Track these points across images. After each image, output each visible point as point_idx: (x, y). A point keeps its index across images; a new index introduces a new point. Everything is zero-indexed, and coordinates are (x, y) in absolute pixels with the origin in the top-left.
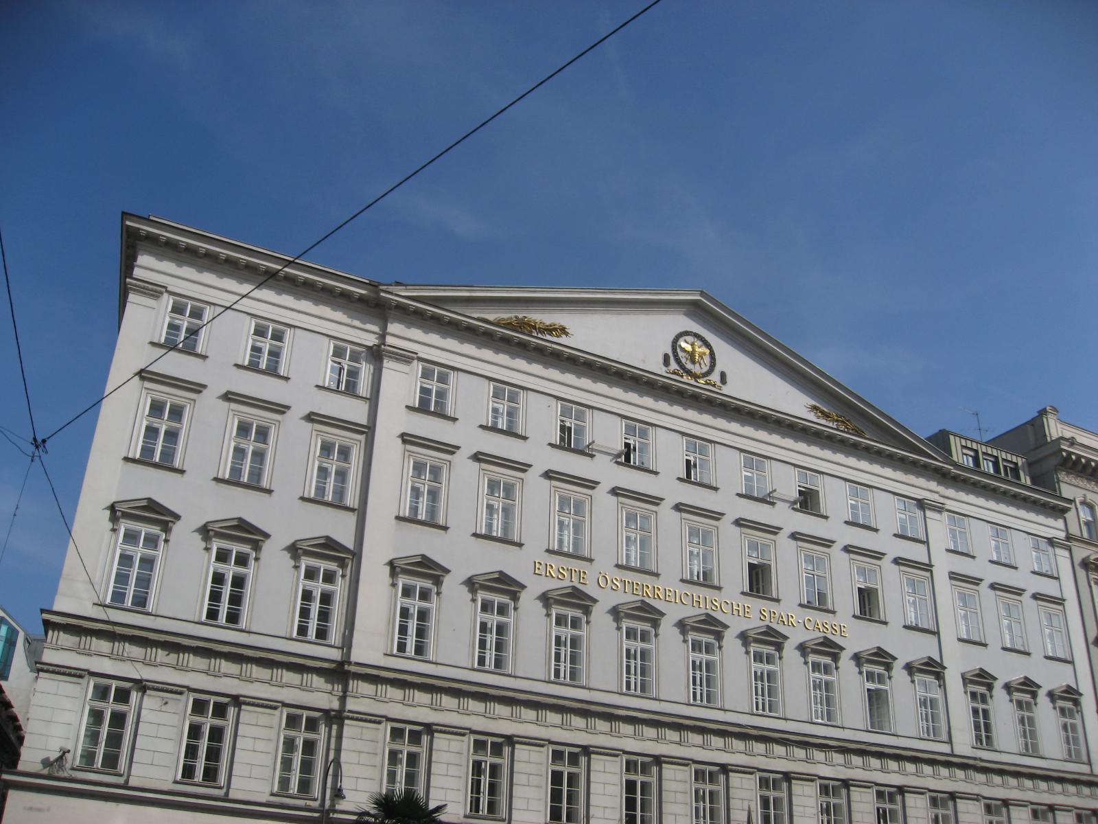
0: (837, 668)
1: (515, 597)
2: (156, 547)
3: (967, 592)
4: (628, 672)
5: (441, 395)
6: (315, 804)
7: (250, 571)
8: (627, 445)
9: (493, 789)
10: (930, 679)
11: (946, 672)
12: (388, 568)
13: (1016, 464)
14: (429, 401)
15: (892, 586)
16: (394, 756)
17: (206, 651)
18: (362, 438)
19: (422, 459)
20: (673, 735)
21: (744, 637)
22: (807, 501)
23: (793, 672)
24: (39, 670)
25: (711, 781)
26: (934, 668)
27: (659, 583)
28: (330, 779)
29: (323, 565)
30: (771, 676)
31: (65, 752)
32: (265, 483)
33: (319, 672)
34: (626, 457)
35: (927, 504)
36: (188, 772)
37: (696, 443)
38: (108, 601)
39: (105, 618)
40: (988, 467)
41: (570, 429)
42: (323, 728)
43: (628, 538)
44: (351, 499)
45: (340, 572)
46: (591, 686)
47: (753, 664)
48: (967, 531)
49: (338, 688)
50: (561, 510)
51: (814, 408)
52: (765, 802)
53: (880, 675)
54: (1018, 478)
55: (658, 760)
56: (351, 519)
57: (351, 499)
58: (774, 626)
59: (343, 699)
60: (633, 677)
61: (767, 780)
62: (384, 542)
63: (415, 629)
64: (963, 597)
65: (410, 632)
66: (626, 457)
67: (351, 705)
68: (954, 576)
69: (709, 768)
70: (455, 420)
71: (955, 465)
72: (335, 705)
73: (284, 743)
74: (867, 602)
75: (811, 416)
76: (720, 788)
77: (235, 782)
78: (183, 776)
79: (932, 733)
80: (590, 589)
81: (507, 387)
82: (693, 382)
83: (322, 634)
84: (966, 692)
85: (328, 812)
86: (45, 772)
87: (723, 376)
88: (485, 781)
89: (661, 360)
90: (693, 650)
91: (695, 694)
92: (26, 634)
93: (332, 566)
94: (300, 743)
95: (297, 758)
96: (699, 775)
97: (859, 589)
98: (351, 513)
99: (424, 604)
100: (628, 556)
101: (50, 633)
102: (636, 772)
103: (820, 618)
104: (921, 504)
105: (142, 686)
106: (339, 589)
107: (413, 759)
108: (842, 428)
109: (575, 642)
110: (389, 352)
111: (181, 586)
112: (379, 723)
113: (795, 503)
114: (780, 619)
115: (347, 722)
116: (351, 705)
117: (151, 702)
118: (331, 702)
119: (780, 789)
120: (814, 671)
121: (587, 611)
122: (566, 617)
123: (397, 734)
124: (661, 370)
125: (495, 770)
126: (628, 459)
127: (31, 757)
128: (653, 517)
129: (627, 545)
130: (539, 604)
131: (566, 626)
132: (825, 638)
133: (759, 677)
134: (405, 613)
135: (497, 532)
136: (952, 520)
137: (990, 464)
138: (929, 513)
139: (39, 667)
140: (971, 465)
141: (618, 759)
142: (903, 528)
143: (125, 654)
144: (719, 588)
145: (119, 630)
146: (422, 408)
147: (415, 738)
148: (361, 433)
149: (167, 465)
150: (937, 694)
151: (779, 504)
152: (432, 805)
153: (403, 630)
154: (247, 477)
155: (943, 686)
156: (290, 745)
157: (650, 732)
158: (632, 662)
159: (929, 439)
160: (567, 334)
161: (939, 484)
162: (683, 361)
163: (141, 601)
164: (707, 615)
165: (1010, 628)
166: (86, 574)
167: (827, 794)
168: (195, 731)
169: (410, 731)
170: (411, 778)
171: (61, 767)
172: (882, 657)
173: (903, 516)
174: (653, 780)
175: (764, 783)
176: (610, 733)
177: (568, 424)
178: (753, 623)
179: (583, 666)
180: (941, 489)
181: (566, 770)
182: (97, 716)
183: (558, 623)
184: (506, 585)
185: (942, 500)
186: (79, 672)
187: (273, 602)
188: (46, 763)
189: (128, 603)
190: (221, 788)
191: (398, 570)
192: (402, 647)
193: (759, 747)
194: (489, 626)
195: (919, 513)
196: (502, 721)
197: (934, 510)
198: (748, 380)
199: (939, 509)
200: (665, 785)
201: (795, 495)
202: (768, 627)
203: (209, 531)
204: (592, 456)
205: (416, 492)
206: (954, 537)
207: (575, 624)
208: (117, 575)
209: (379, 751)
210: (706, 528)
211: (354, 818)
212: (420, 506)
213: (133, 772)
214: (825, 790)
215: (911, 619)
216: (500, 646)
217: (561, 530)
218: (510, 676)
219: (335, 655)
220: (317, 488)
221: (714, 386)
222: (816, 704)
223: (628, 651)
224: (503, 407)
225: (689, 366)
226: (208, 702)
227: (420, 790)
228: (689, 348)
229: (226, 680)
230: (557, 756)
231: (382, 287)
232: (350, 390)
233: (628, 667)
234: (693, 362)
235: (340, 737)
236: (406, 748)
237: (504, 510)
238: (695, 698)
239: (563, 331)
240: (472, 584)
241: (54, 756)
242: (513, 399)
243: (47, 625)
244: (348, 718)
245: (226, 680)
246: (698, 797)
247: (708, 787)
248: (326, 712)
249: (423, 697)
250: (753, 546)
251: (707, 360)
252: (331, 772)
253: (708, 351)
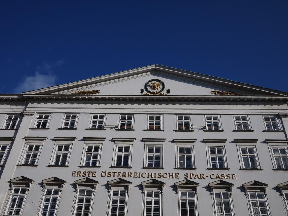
35: (281, 115)
89: (140, 91)
103: (220, 173)
114: (196, 176)
138: (283, 119)
151: (196, 130)
160: (99, 92)
162: (150, 90)
184: (58, 182)
225: (153, 91)
231: (23, 94)
234: (154, 89)
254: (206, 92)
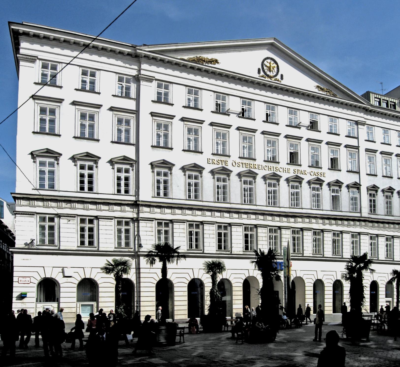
0: (321, 189)
1: (201, 172)
2: (54, 167)
3: (371, 156)
4: (245, 196)
5: (166, 94)
6: (132, 250)
7: (94, 172)
8: (243, 109)
9: (197, 240)
10: (355, 190)
11: (361, 187)
12: (150, 166)
13: (395, 103)
14: (161, 97)
15: (343, 156)
16: (159, 232)
17: (82, 201)
18: (134, 115)
19: (160, 122)
20: (261, 217)
21: (287, 180)
22: (313, 126)
23: (306, 191)
24: (15, 214)
25: (275, 232)
26: (357, 186)
27: (256, 163)
28: (136, 241)
29: (124, 167)
30: (297, 194)
31: (33, 241)
32: (96, 137)
33: (128, 205)
34: (242, 114)
36: (82, 243)
37: (271, 106)
38: (38, 188)
39: (39, 194)
40: (384, 105)
41: (220, 104)
42: (131, 224)
43: (244, 147)
44: (133, 140)
45: (131, 168)
46: (231, 202)
47: (291, 190)
48: (374, 132)
49: (135, 210)
50: (217, 138)
52: (294, 239)
53: (337, 190)
54: (395, 108)
55: (256, 226)
56: (133, 148)
57: (133, 140)
58: (299, 175)
59: (138, 214)
60: (246, 198)
61: (295, 231)
62: (148, 155)
63: (163, 187)
64: (370, 158)
65: (161, 188)
66: (242, 114)
67: (141, 215)
68: (367, 150)
69: (274, 228)
70: (172, 105)
71: (372, 106)
72: (135, 216)
73: (117, 231)
74: (334, 164)
75: (316, 90)
76: (278, 235)
77: (101, 245)
78: (81, 244)
79: (355, 210)
80: (230, 167)
81: (194, 89)
82: (269, 80)
83: (127, 192)
84: (368, 194)
85: (137, 252)
86: (27, 247)
87: (282, 76)
88: (194, 237)
90: (269, 186)
91: (269, 202)
92: (7, 203)
93: (128, 167)
94: (123, 230)
95: (123, 235)
96: (271, 231)
97: (331, 159)
98: (133, 146)
99: (166, 178)
100: (244, 154)
101: (17, 201)
102: (248, 231)
104: (357, 123)
105: (59, 216)
106: (132, 175)
107: (166, 232)
108: (328, 94)
109: (224, 187)
110: (143, 77)
111: (67, 179)
112: (153, 221)
113: (308, 127)
115: (140, 221)
116: (141, 215)
117: (63, 221)
118: (133, 215)
119: (299, 234)
120: (313, 190)
121: (228, 175)
122: (220, 178)
123: (159, 224)
124: (257, 76)
125: (197, 233)
126: (243, 115)
127: (19, 243)
128: (253, 137)
129: (243, 149)
130: (210, 174)
131: (221, 181)
132: (318, 178)
133: (292, 194)
134: (158, 182)
135: (192, 148)
136: (368, 128)
137: (385, 104)
138: (359, 126)
139: (15, 213)
140: (378, 105)
141: (241, 227)
142: (349, 133)
143: (49, 205)
144: (278, 163)
145: (45, 197)
146: (159, 101)
147: (167, 225)
148: (134, 113)
149: (52, 133)
150: (357, 196)
151: (302, 128)
152: (175, 247)
153: (158, 188)
154: (88, 134)
155: (360, 192)
156: (119, 231)
157: (253, 217)
158: (246, 192)
159: (362, 96)
160: (218, 63)
161: (364, 114)
162: (266, 71)
163: (52, 187)
164: (274, 173)
165: (386, 168)
166: (26, 179)
167: (316, 235)
168: (82, 229)
169: (164, 223)
170: (166, 238)
171: (33, 245)
172: (338, 183)
173: (349, 128)
174: (254, 233)
175: (294, 232)
176: (238, 218)
177: (219, 103)
178: (291, 174)
179: (228, 196)
180: (365, 116)
181: (223, 232)
182: (43, 228)
183: (218, 181)
185: (365, 120)
186: (32, 213)
187: (105, 182)
188: (26, 244)
189: (47, 187)
190: (96, 247)
191: (154, 166)
192: (158, 194)
193: (292, 220)
194: (192, 184)
195: (355, 126)
196: (198, 217)
199: (363, 124)
200: (259, 234)
201: (308, 123)
202: (297, 175)
203: (75, 158)
204: (229, 115)
205: (159, 136)
206: (368, 135)
207: (224, 180)
208: (40, 178)
209: (154, 230)
210: (274, 140)
211: (147, 253)
212: (161, 141)
213: (61, 245)
214: (315, 233)
215: (350, 168)
216: (196, 191)
217: (217, 146)
218: (200, 201)
219: (133, 198)
220: (118, 137)
221: (278, 81)
222: (313, 202)
223: (244, 189)
224: (192, 97)
225: (268, 73)
226: (86, 219)
227: (170, 242)
228: (268, 65)
229: (92, 211)
230: (220, 227)
232: (127, 96)
233: (245, 195)
234: (270, 71)
235: (138, 227)
236: (163, 229)
237: (194, 140)
238: (269, 204)
239: (216, 61)
240: (183, 169)
241: (29, 242)
242: (196, 93)
243: (15, 198)
244: (141, 220)
245: (92, 211)
246: (270, 238)
247: (274, 235)
248: (132, 219)
249: (168, 211)
250: (292, 145)
251: (276, 69)
252: (136, 239)
253: (276, 66)
254: (309, 84)
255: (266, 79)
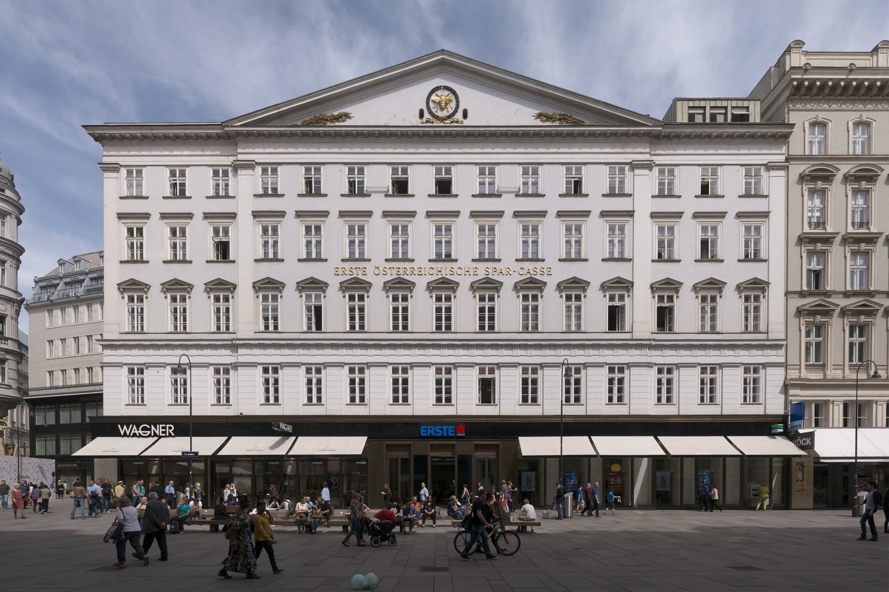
51: (539, 116)
75: (538, 122)
82: (442, 124)
124: (416, 121)
160: (349, 118)
162: (434, 111)
197: (642, 168)
198: (484, 108)
221: (457, 122)
234: (442, 109)
255: (435, 124)
